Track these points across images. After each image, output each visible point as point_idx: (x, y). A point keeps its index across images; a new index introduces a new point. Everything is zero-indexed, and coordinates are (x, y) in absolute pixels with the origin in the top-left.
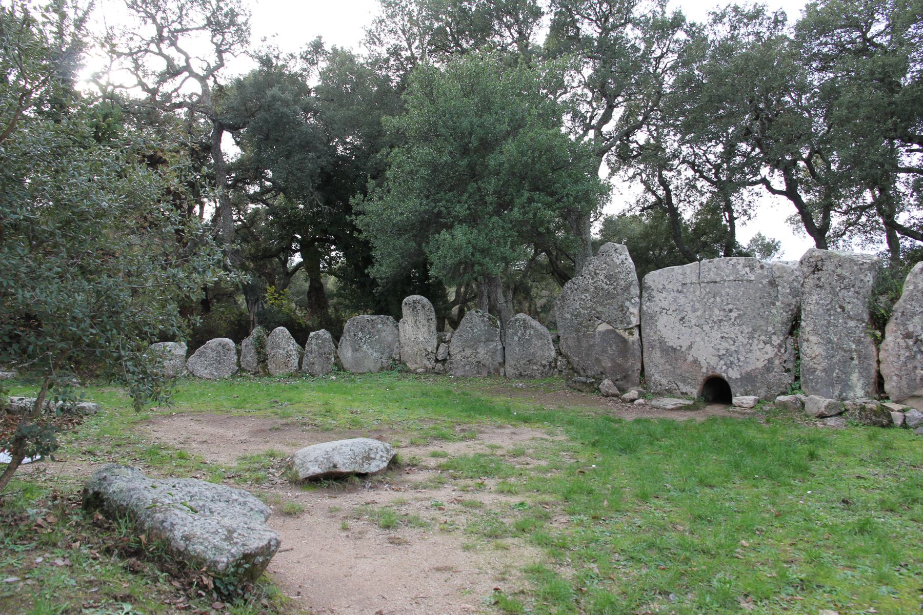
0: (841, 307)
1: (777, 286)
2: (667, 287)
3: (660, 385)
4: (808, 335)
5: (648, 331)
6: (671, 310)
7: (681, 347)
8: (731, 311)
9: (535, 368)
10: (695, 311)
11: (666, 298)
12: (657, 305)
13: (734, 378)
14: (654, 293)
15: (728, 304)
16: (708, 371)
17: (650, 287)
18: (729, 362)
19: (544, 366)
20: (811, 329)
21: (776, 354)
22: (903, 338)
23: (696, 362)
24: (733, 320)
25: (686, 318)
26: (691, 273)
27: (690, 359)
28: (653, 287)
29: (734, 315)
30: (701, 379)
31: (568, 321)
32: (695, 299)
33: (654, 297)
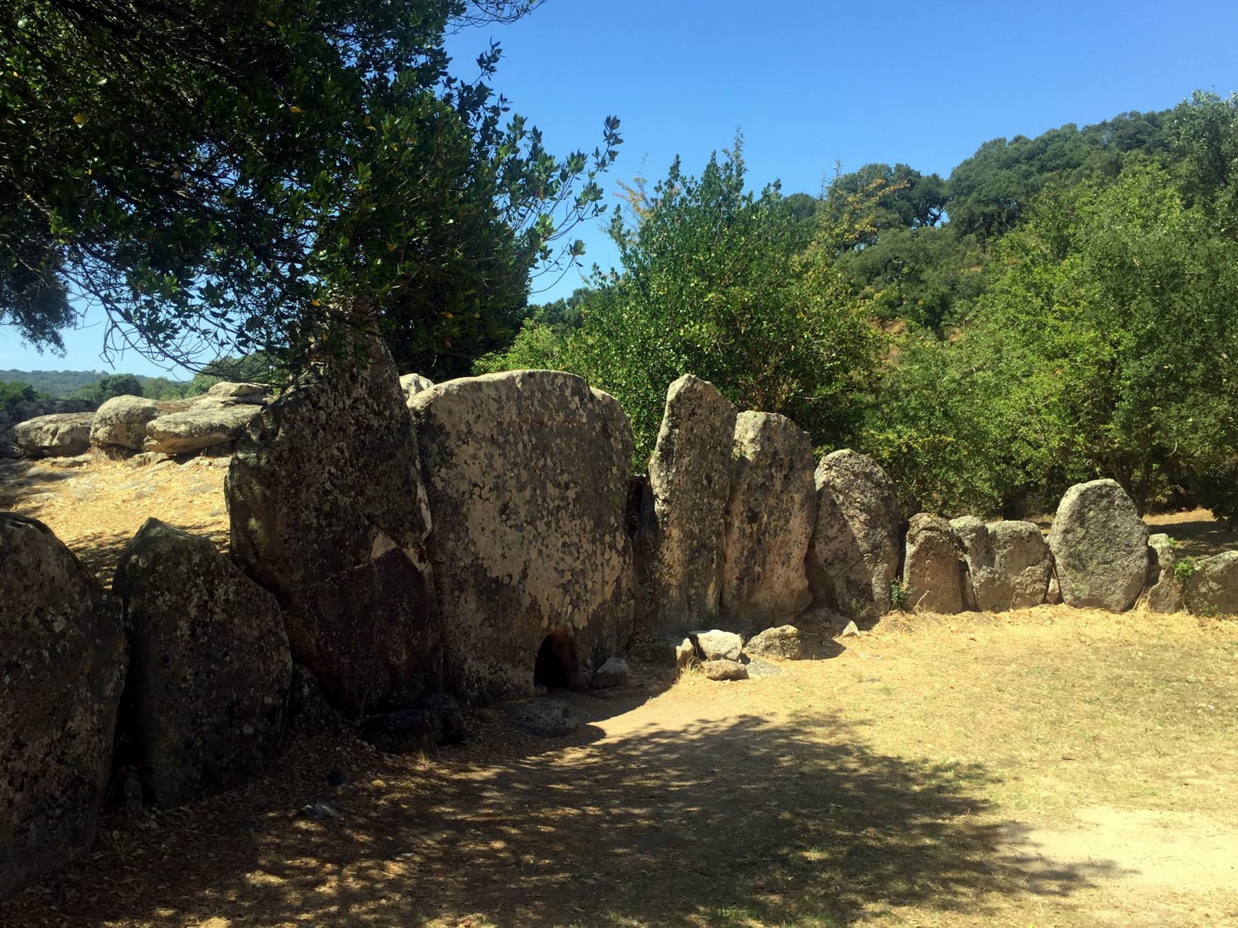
0: (709, 479)
1: (610, 436)
2: (475, 429)
3: (479, 680)
4: (671, 528)
5: (451, 544)
6: (487, 488)
7: (510, 576)
8: (567, 487)
9: (248, 730)
10: (521, 489)
11: (474, 457)
12: (463, 477)
13: (581, 628)
14: (452, 443)
15: (562, 472)
16: (550, 624)
17: (442, 427)
18: (574, 598)
19: (270, 713)
20: (676, 515)
21: (623, 569)
22: (749, 523)
23: (534, 607)
24: (571, 506)
25: (511, 504)
26: (508, 400)
27: (526, 601)
28: (448, 428)
29: (571, 494)
30: (538, 644)
31: (312, 535)
32: (518, 460)
33: (452, 454)
